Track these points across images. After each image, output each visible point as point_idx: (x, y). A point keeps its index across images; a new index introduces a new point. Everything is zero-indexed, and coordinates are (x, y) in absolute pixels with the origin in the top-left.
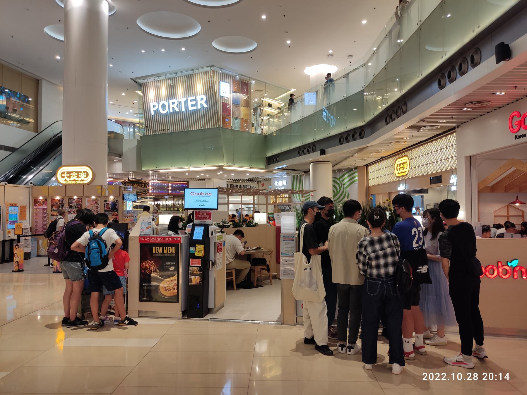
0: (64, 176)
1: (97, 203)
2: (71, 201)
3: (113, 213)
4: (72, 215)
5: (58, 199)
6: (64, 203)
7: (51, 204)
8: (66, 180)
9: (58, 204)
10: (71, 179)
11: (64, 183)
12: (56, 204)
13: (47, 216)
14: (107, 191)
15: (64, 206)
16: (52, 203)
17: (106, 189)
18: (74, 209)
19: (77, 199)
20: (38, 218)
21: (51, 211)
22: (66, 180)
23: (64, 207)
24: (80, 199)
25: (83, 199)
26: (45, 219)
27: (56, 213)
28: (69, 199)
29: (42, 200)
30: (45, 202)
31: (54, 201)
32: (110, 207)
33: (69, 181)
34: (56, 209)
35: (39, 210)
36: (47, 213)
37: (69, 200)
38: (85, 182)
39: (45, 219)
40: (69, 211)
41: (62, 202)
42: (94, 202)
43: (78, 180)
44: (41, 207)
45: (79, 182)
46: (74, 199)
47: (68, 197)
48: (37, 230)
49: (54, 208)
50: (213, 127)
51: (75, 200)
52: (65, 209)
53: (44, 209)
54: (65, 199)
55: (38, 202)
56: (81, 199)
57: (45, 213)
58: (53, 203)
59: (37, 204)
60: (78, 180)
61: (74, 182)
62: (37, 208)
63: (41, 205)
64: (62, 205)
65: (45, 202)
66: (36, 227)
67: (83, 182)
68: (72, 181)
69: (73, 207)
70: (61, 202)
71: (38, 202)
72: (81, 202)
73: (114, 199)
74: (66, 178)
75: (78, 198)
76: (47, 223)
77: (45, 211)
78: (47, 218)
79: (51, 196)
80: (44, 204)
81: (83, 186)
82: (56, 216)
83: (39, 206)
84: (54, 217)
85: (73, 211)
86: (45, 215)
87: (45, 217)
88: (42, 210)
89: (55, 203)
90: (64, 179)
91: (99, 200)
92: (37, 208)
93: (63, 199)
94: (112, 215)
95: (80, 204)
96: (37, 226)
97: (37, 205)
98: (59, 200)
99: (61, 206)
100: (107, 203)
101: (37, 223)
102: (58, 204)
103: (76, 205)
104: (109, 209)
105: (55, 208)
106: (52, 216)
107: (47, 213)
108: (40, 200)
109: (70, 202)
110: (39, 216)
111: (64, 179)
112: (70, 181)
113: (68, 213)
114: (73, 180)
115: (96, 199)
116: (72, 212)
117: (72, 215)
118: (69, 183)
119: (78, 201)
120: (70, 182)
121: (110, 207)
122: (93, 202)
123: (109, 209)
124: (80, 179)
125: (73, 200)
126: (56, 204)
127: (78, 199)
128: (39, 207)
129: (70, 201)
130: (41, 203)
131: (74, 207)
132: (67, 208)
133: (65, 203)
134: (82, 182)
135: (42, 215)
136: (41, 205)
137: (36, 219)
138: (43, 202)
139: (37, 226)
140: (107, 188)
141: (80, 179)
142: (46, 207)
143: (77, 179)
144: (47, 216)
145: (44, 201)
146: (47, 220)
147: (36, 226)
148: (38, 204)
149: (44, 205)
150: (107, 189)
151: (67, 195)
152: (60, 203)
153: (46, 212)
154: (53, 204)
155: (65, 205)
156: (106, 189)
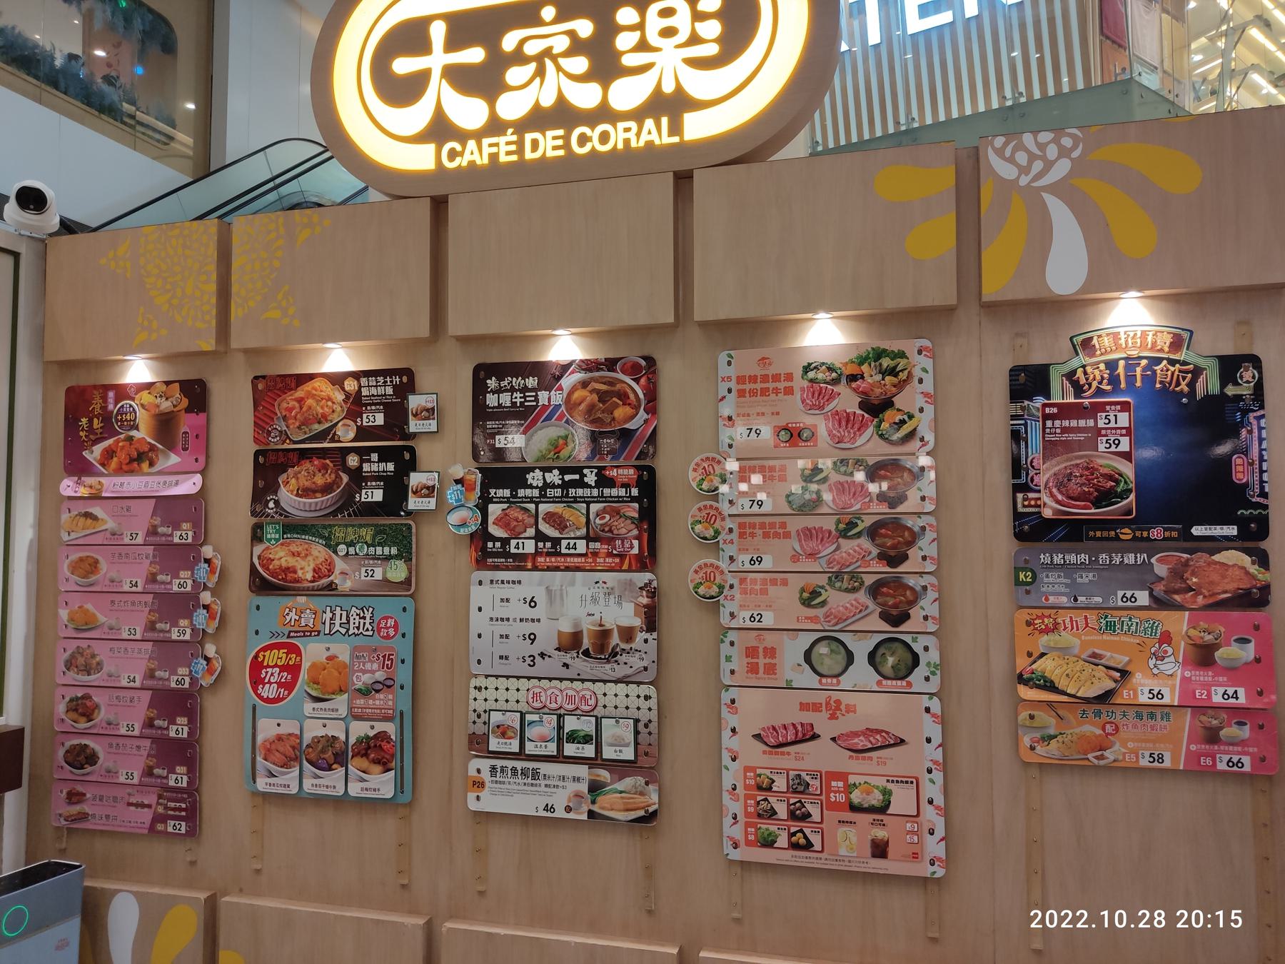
0: (418, 83)
1: (890, 416)
2: (506, 399)
3: (1178, 573)
4: (525, 591)
5: (337, 379)
6: (414, 426)
7: (249, 448)
8: (440, 130)
9: (346, 434)
10: (512, 106)
11: (421, 159)
12: (321, 436)
13: (206, 597)
14: (1059, 211)
15: (412, 465)
16: (262, 425)
17: (1053, 203)
18: (543, 508)
19: (588, 366)
20: (102, 619)
21: (257, 535)
22: (440, 130)
23: (415, 479)
24: (634, 370)
25: (671, 372)
26: (180, 632)
27: (319, 551)
28: (482, 373)
29: (146, 397)
30: (187, 423)
31: (289, 401)
32: (1128, 470)
33: (478, 135)
34: (320, 499)
35: (110, 524)
36: (207, 551)
37: (479, 389)
38: (698, 127)
39: (180, 632)
40: (481, 537)
41: (397, 413)
42: (847, 400)
43: (604, 113)
44: (133, 484)
45: (620, 135)
46: (549, 375)
47: (465, 340)
48: (92, 759)
49: (287, 496)
50: (1080, 86)
51: (568, 381)
52: (431, 503)
53: (170, 508)
54: (424, 378)
55: (106, 417)
56: (647, 369)
57: (186, 556)
58: (285, 436)
59: (98, 449)
60: (604, 113)
61: (548, 144)
62: (96, 497)
63: (139, 459)
64: (385, 455)
65: (187, 423)
66: (83, 725)
67: (676, 128)
68: (523, 126)
69: (535, 478)
70: (380, 419)
71: (109, 431)
72: (652, 408)
73: (1176, 344)
74: (441, 94)
75: (601, 356)
76: (206, 681)
77: (185, 534)
78: (200, 617)
79: (253, 343)
80: (171, 447)
81: (683, 179)
82: (311, 592)
83: (120, 471)
84: (288, 601)
85: (540, 537)
86: (181, 583)
87: (184, 605)
88: (143, 516)
89: (305, 423)
90: (417, 116)
91: (920, 364)
92: (96, 497)
93: (405, 381)
94: (1160, 603)
95: (626, 435)
96: (88, 716)
97: (94, 454)
98: (351, 385)
99: (373, 466)
100: (1066, 411)
101: (93, 679)
102: (346, 434)
103: (580, 449)
104: (1104, 497)
105: (305, 492)
106: (269, 602)
107: (207, 551)
108: (122, 392)
109: (503, 414)
110: (112, 593)
111: (417, 116)
112: (495, 126)
113: (466, 556)
114: (538, 119)
115: (879, 354)
116: (530, 547)
117: (525, 591)
118: (474, 155)
119: (611, 396)
120: (503, 148)
121: (1115, 477)
122: (819, 396)
123: (1104, 497)
124: (628, 93)
125: (532, 382)
126: (321, 436)
127: (611, 364)
128: (112, 484)
129: (491, 400)
130: (143, 433)
131: (554, 477)
132: (452, 494)
133: (432, 425)
134: (655, 134)
135: (152, 579)
136: (140, 457)
137: (84, 625)
138: (165, 425)
139: (88, 716)
140: (1062, 168)
141: (628, 93)
142: (189, 485)
143: (586, 96)
144: (206, 597)
145: (166, 405)
146: (210, 650)
147: (82, 708)
148: (109, 454)
149: (174, 459)
150: (1053, 189)
151: (456, 324)
152: (362, 433)
153: (195, 547)
154: (275, 443)
155: (424, 450)
156: (1053, 203)
